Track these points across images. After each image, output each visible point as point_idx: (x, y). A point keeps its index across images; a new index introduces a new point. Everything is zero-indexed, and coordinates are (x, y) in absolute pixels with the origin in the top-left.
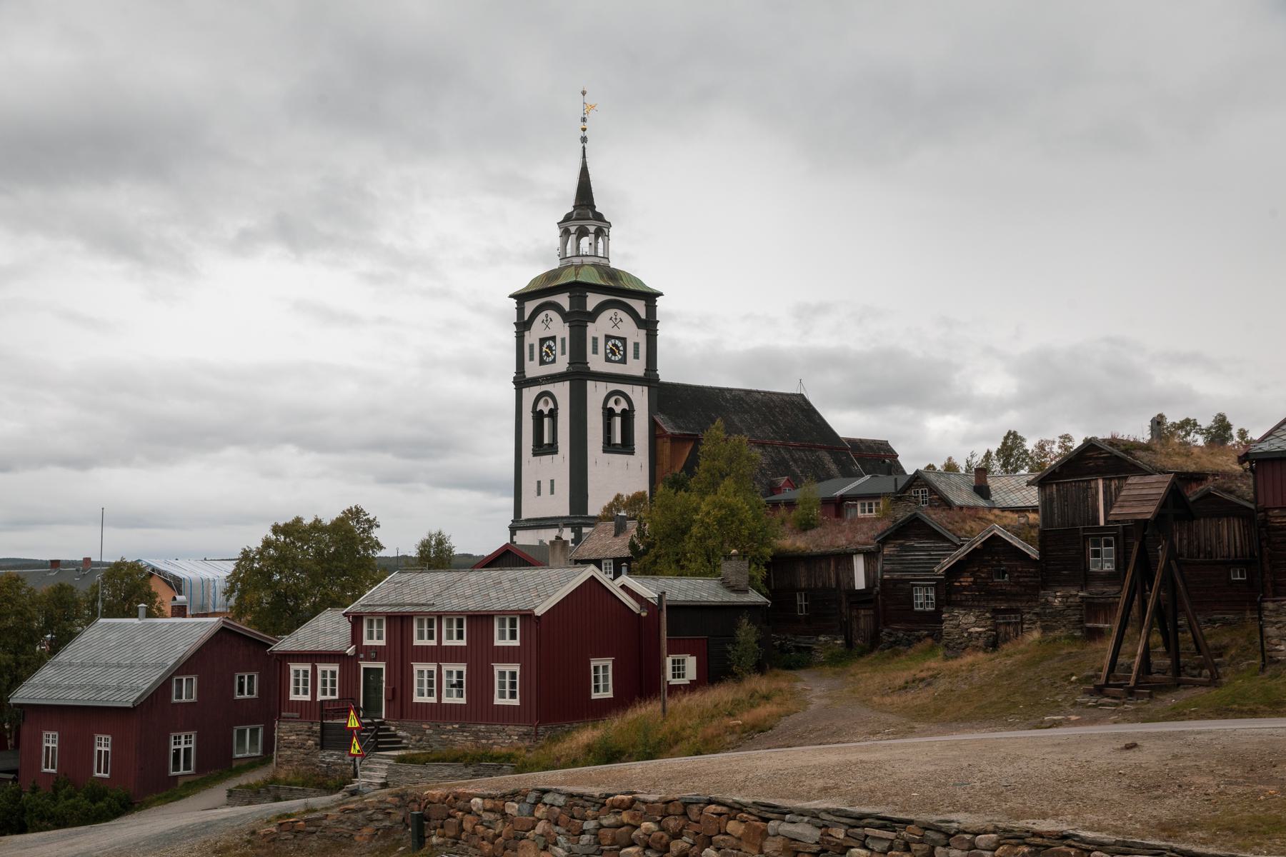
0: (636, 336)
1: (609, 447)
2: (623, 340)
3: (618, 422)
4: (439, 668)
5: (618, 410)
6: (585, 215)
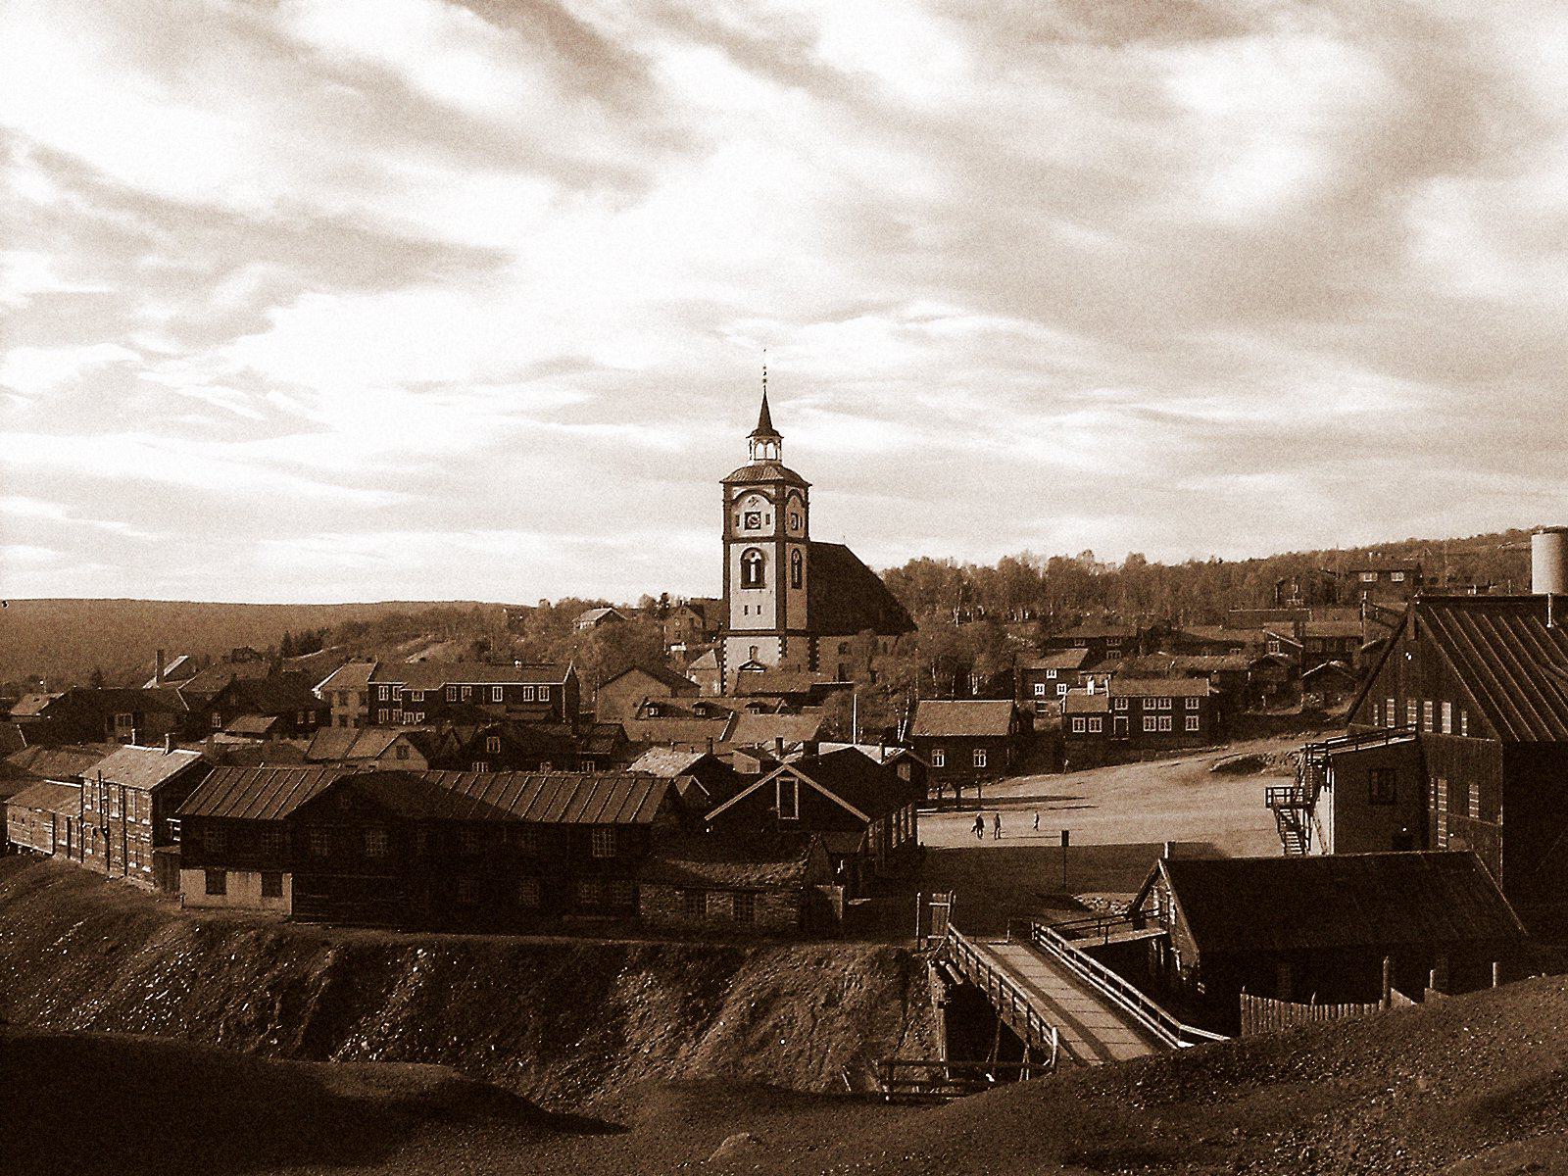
0: (768, 509)
1: (746, 584)
2: (759, 513)
3: (753, 566)
4: (1157, 718)
5: (753, 560)
6: (766, 431)
